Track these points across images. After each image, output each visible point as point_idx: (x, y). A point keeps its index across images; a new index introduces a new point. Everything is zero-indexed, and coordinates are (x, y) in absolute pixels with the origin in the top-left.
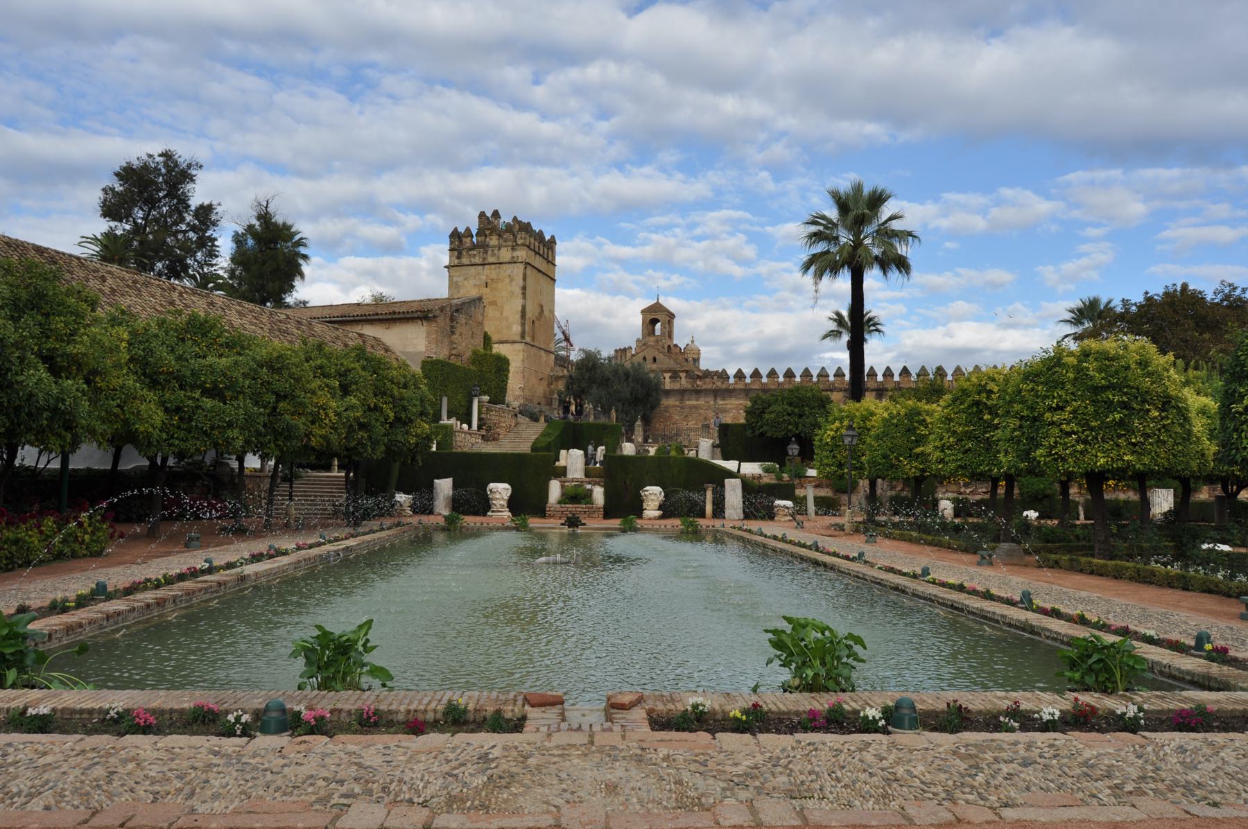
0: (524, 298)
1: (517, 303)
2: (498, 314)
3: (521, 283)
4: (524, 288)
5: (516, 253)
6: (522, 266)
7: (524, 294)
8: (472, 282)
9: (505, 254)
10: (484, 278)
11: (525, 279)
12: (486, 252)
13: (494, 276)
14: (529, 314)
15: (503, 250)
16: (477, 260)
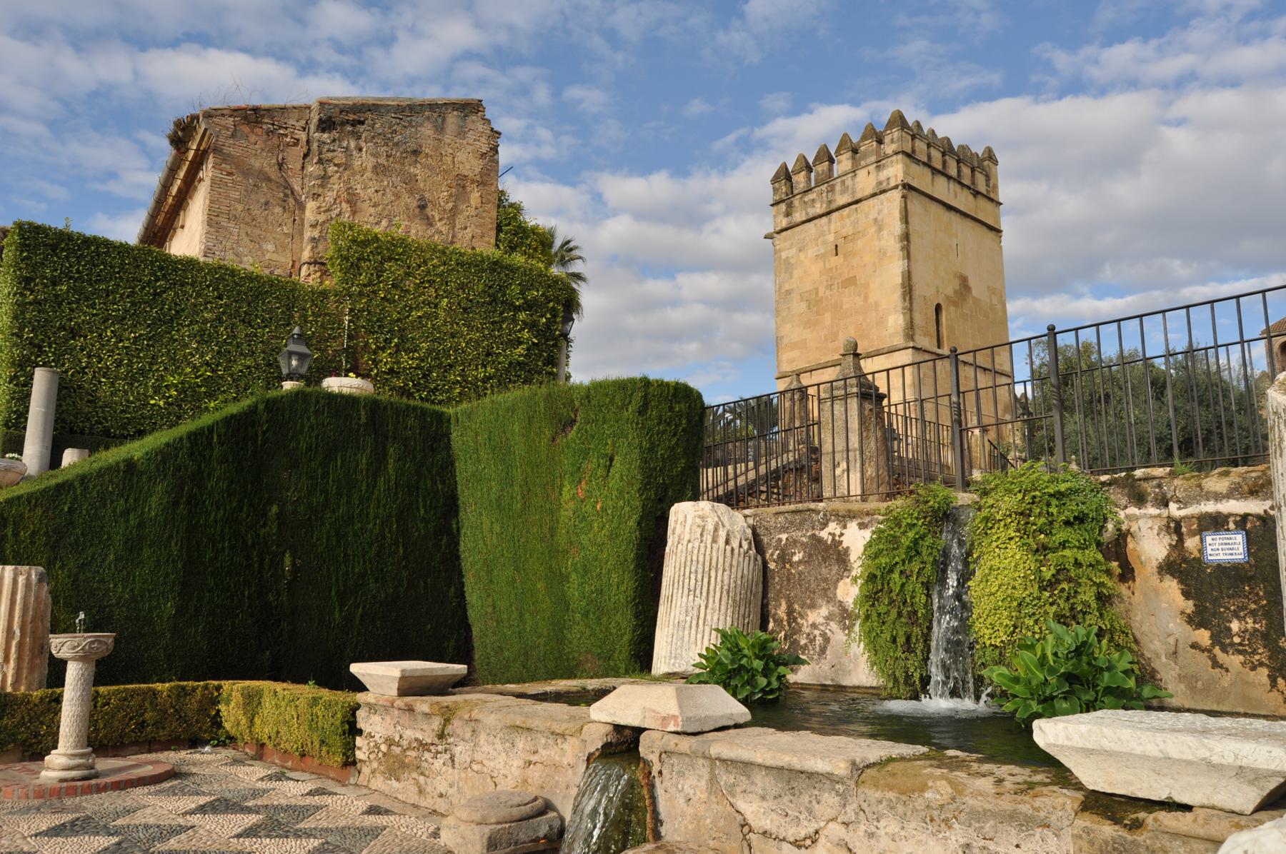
0: (908, 256)
1: (895, 269)
2: (859, 301)
3: (897, 227)
4: (906, 237)
5: (884, 174)
6: (896, 195)
7: (908, 254)
8: (811, 252)
9: (865, 181)
10: (831, 238)
11: (905, 218)
12: (832, 189)
13: (848, 230)
14: (927, 290)
15: (862, 174)
16: (819, 208)
